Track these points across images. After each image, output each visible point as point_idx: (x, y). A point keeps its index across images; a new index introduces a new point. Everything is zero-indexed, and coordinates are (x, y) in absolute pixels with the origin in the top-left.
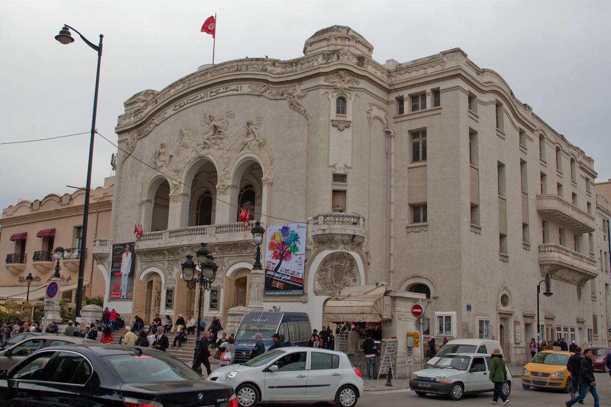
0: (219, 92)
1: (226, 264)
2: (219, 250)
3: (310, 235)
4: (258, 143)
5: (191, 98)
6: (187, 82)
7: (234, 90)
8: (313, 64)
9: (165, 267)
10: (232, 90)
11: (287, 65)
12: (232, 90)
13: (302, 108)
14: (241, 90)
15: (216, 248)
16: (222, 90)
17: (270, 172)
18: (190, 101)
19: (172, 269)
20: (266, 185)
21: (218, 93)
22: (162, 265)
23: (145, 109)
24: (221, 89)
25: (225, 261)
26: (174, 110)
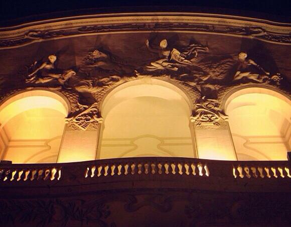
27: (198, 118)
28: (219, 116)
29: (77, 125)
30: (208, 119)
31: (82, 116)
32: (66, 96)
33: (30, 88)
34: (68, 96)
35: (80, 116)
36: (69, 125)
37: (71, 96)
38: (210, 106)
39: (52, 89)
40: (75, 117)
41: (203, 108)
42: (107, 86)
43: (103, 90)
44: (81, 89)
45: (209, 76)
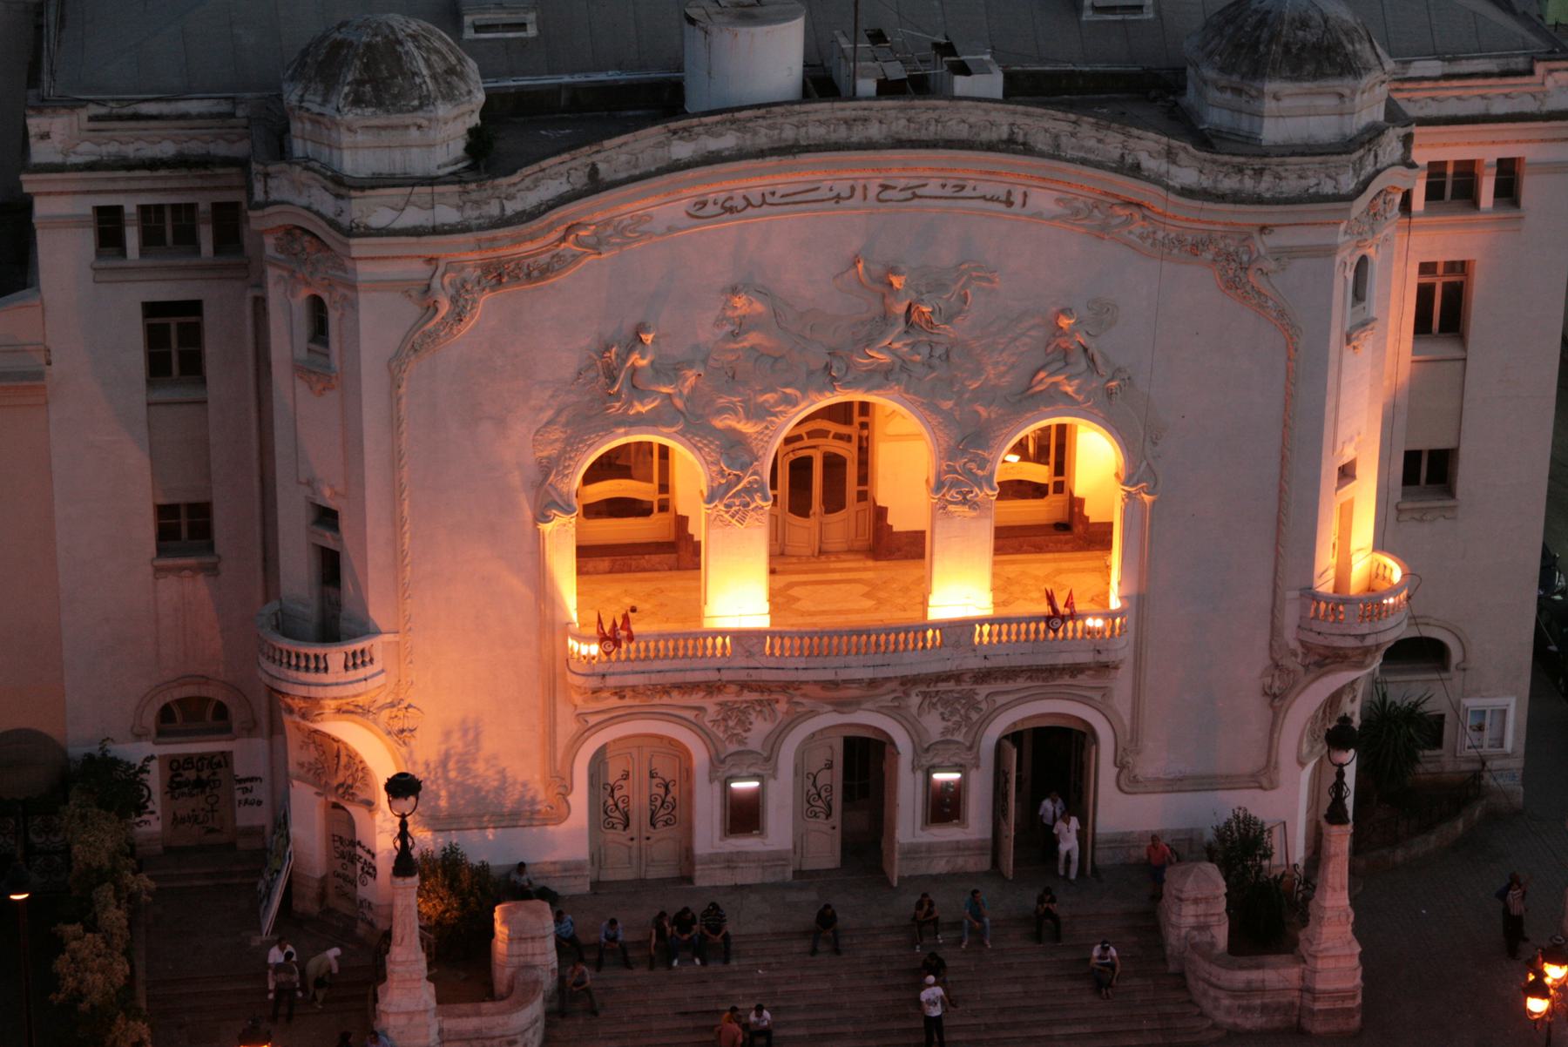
0: (919, 192)
1: (984, 706)
3: (1290, 637)
5: (781, 190)
6: (763, 131)
7: (998, 200)
8: (1318, 184)
9: (706, 719)
10: (984, 198)
11: (1225, 169)
12: (984, 198)
14: (1024, 204)
17: (1148, 464)
18: (775, 200)
19: (746, 725)
21: (915, 196)
22: (690, 715)
23: (528, 189)
25: (979, 698)
26: (689, 214)
27: (944, 495)
28: (981, 489)
29: (727, 516)
30: (961, 498)
31: (734, 496)
32: (695, 446)
33: (622, 430)
34: (700, 445)
35: (730, 498)
36: (712, 518)
37: (706, 445)
38: (972, 465)
39: (665, 430)
40: (721, 499)
41: (956, 472)
42: (773, 418)
43: (767, 428)
44: (720, 423)
45: (983, 377)
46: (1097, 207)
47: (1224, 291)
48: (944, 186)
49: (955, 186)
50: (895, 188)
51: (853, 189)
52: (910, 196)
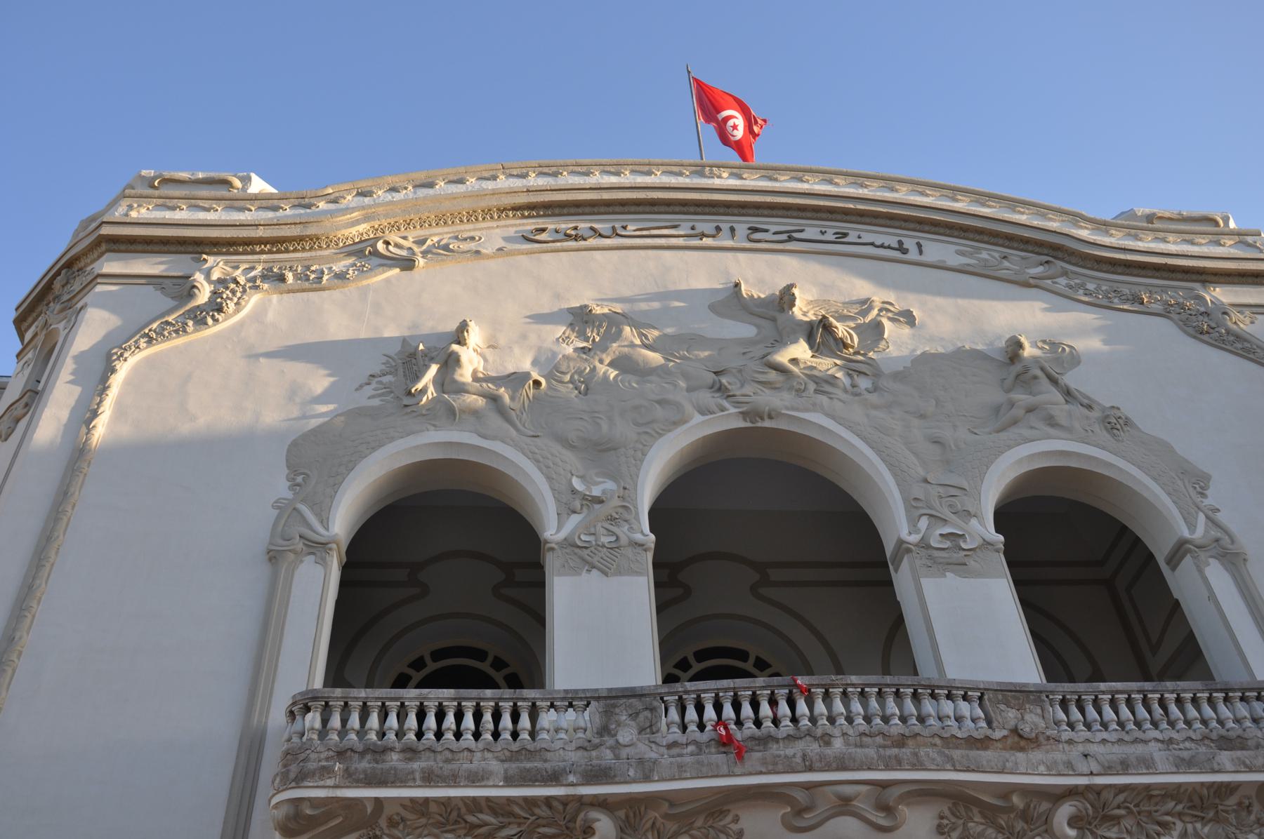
0: (795, 235)
2: (1072, 822)
4: (1096, 414)
7: (889, 247)
10: (872, 244)
12: (872, 244)
13: (1259, 351)
14: (921, 252)
15: (1065, 810)
16: (811, 233)
17: (1207, 517)
20: (1211, 560)
21: (791, 239)
24: (811, 233)
46: (1005, 257)
47: (1195, 337)
48: (823, 233)
49: (834, 234)
50: (767, 231)
51: (718, 229)
52: (786, 238)
